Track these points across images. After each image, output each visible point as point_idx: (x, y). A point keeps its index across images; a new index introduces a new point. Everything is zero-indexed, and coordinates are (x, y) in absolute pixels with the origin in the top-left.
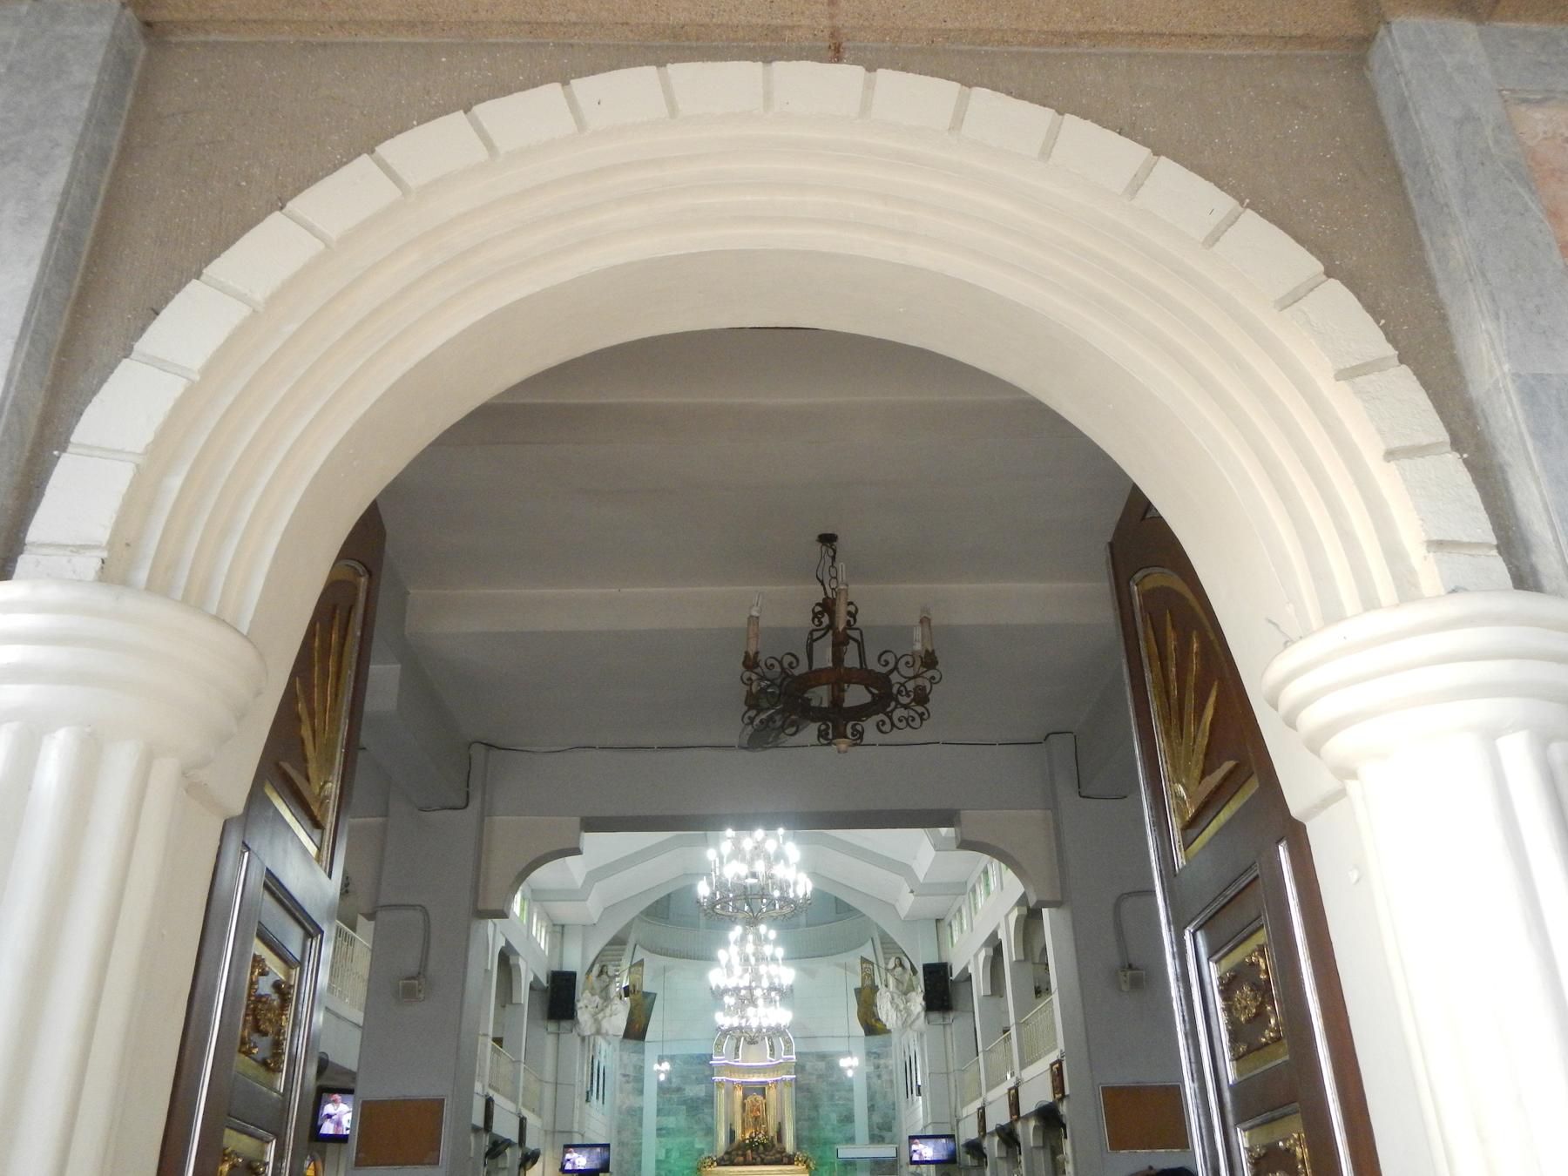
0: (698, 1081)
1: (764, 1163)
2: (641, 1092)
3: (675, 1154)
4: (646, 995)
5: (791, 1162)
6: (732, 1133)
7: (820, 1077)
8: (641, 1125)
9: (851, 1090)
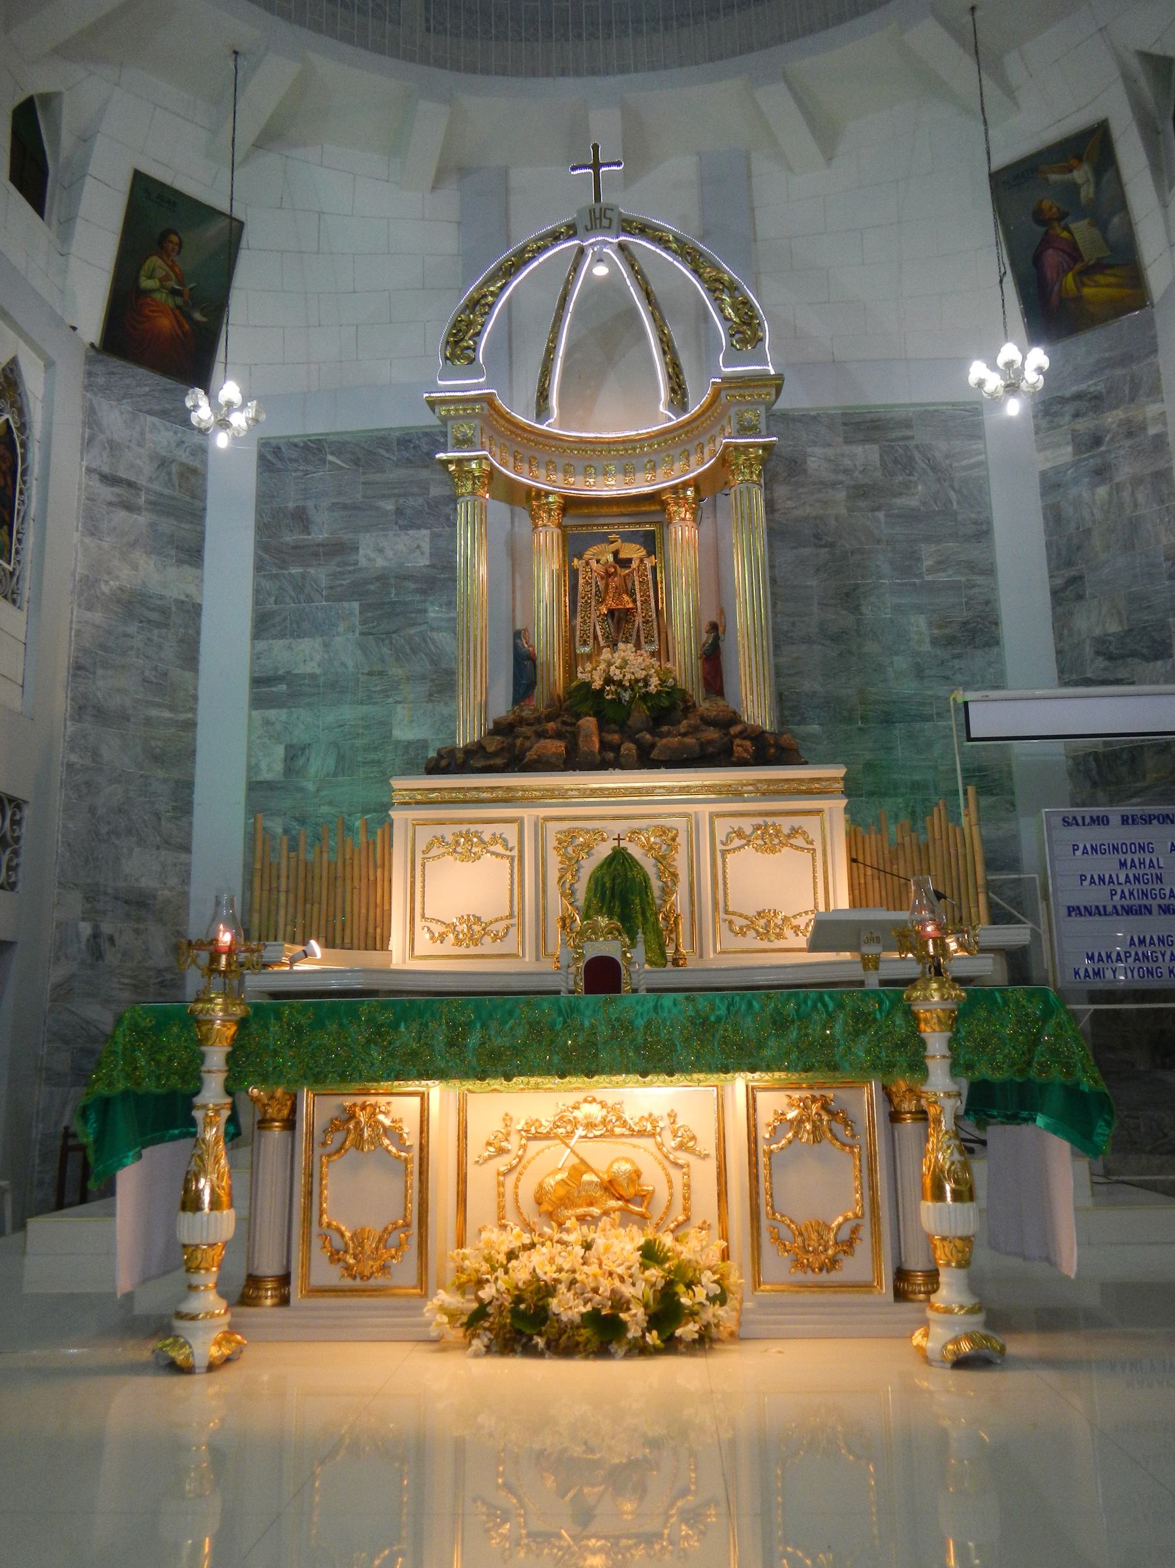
0: (406, 520)
1: (646, 760)
2: (193, 554)
3: (318, 764)
4: (202, 212)
5: (767, 750)
6: (525, 667)
7: (860, 492)
8: (190, 657)
9: (982, 533)
